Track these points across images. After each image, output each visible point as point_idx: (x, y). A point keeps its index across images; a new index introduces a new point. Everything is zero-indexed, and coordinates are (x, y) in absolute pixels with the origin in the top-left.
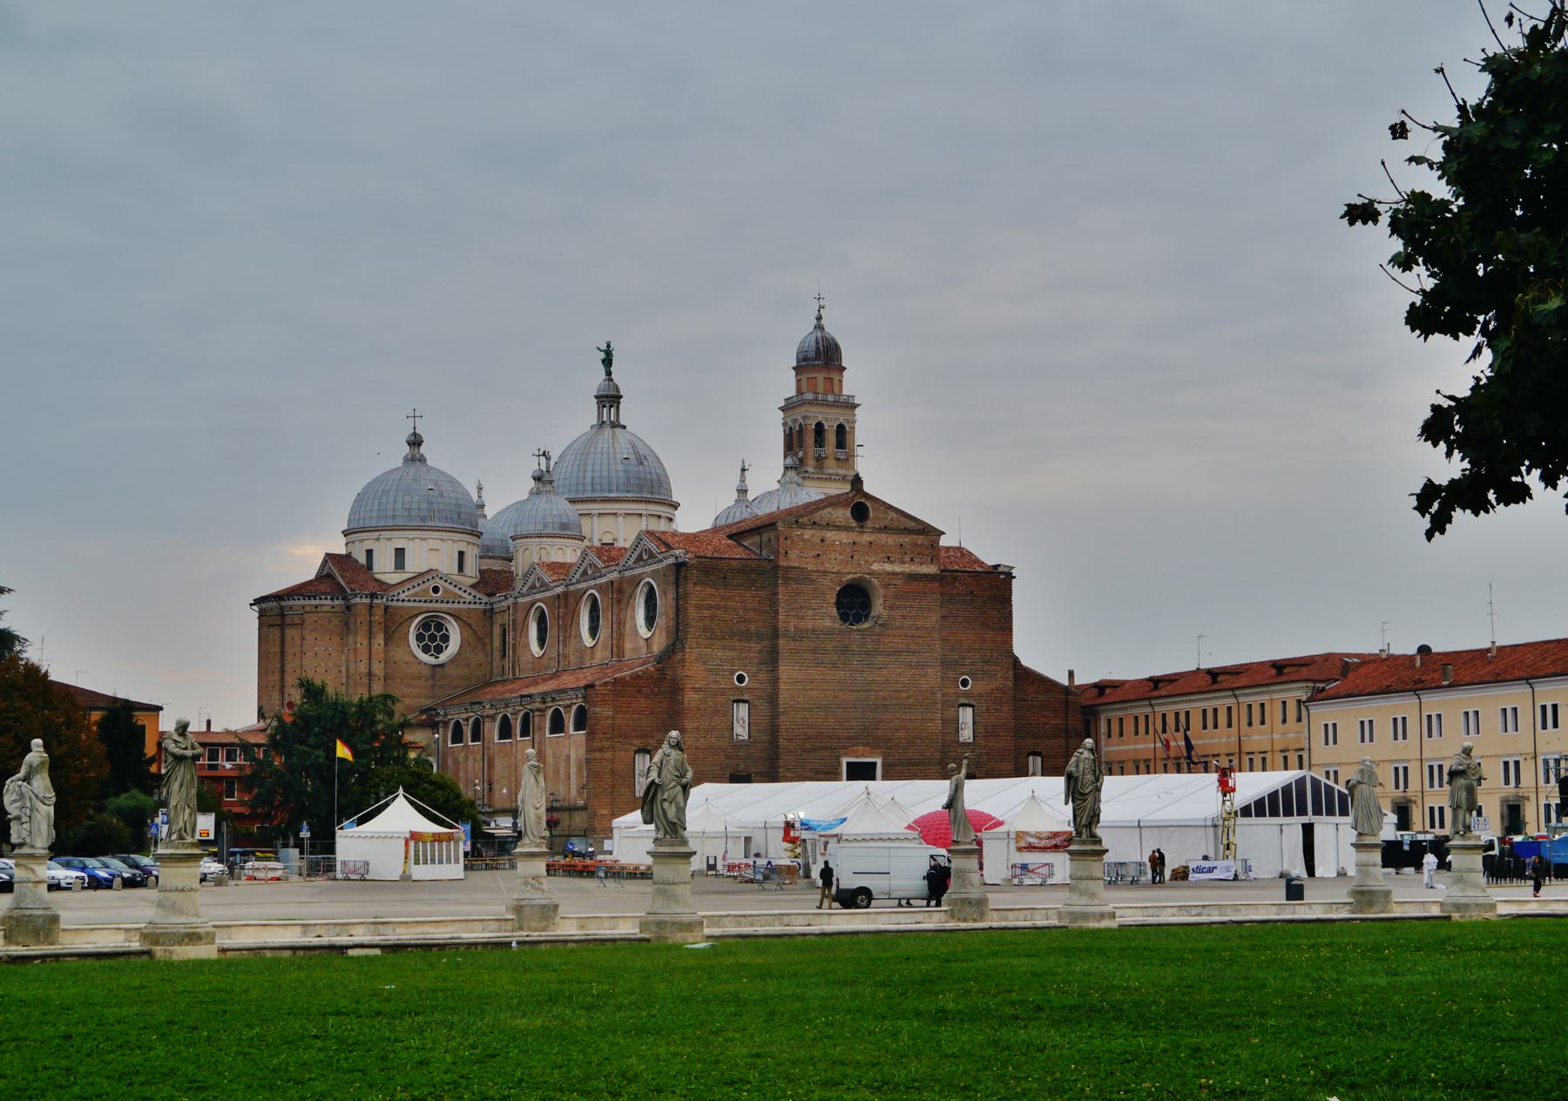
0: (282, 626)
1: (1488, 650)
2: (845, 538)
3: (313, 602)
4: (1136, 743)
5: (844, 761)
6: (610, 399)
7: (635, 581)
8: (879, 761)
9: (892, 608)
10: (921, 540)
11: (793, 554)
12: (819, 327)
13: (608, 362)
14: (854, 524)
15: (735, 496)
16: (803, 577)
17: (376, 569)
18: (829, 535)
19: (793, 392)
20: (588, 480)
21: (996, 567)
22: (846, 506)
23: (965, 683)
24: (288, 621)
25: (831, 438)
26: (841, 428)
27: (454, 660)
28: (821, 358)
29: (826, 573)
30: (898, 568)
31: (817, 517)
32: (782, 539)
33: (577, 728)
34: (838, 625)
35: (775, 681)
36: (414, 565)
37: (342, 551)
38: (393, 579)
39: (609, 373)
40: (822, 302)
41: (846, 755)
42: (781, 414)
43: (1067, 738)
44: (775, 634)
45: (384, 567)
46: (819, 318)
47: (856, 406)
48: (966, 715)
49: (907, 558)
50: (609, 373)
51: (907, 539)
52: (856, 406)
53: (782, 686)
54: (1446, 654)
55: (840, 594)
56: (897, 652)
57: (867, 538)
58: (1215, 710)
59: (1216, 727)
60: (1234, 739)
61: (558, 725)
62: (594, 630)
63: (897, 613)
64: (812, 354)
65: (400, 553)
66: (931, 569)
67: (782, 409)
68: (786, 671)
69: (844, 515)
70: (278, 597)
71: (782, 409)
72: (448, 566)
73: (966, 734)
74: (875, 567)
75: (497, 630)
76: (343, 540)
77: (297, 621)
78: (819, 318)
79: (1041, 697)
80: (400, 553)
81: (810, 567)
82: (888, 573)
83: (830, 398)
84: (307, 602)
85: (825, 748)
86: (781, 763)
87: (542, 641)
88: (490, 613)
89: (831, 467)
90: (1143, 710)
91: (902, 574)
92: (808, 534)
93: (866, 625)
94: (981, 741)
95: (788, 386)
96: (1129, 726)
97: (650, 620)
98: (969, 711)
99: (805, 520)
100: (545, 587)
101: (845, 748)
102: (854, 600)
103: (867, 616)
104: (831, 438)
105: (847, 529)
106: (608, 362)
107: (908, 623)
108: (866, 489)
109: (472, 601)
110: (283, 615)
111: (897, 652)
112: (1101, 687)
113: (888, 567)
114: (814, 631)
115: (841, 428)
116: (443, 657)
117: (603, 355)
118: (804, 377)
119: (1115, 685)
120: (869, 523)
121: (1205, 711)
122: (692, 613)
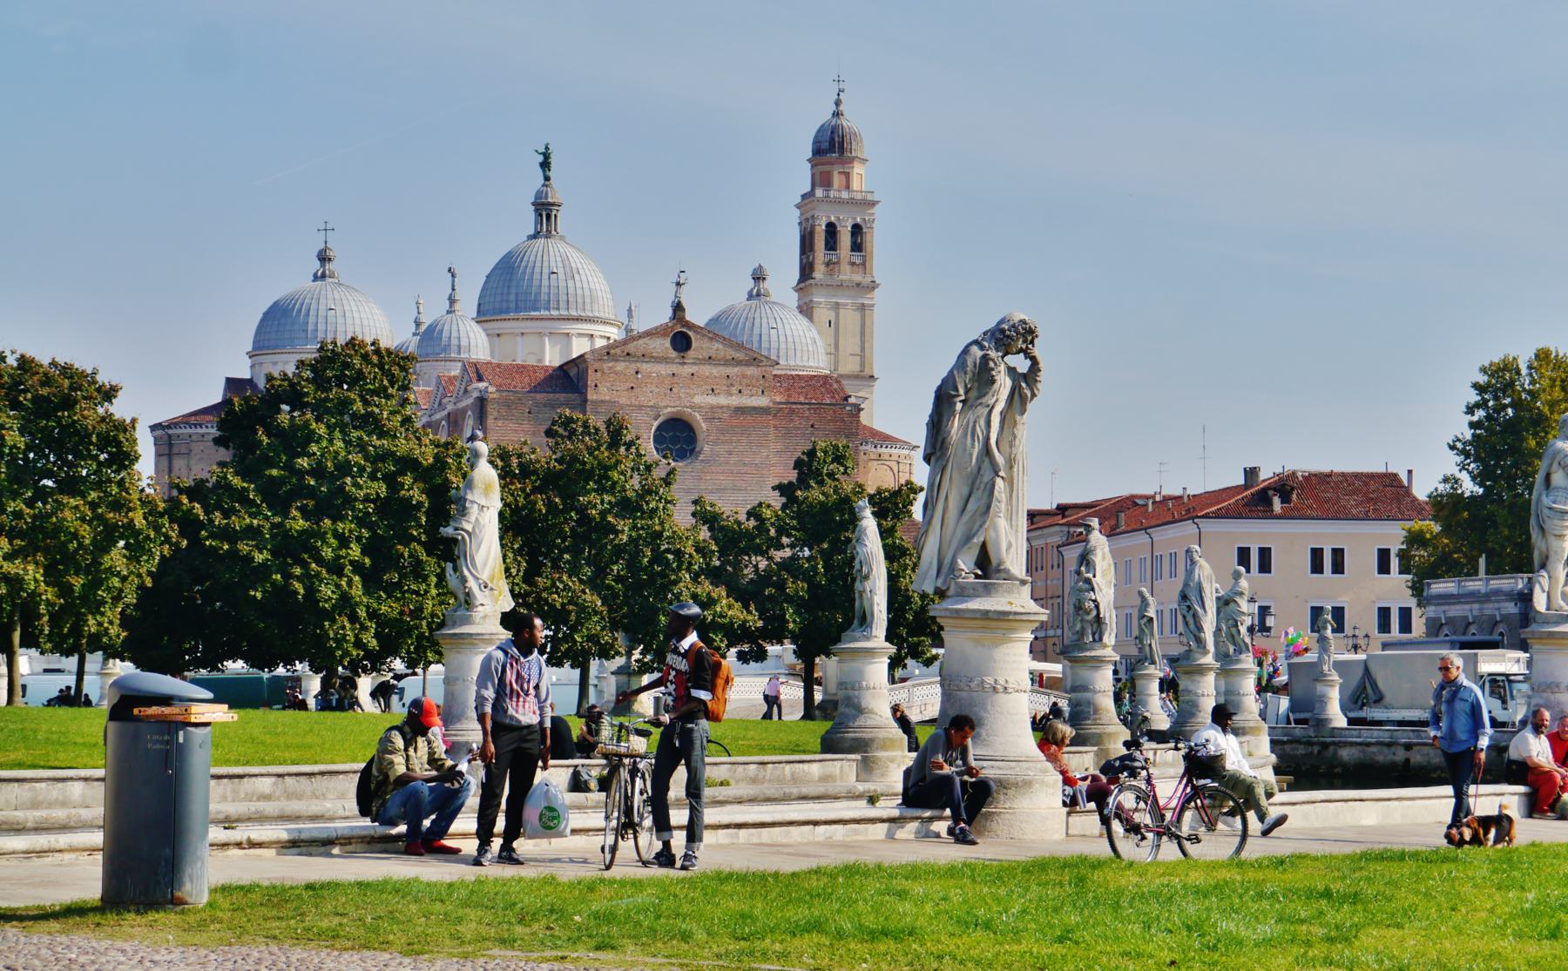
0: (170, 456)
1: (1181, 497)
2: (664, 369)
3: (199, 430)
6: (544, 210)
9: (715, 443)
10: (751, 371)
11: (600, 388)
12: (837, 114)
13: (545, 165)
14: (673, 354)
15: (669, 313)
18: (645, 367)
20: (512, 297)
24: (175, 450)
25: (845, 239)
26: (857, 230)
28: (832, 147)
29: (640, 407)
30: (723, 400)
31: (631, 348)
32: (590, 372)
37: (244, 373)
39: (547, 179)
40: (842, 86)
42: (797, 212)
46: (838, 103)
47: (873, 204)
49: (734, 390)
50: (547, 179)
51: (733, 371)
52: (873, 204)
57: (688, 369)
63: (721, 449)
64: (825, 145)
67: (798, 206)
69: (663, 345)
70: (172, 424)
71: (798, 206)
74: (698, 400)
76: (249, 362)
77: (184, 451)
78: (838, 103)
81: (623, 401)
82: (712, 408)
83: (845, 195)
84: (193, 430)
89: (846, 274)
91: (728, 407)
92: (620, 366)
95: (802, 180)
99: (618, 351)
103: (692, 451)
104: (845, 239)
105: (664, 360)
106: (545, 165)
107: (733, 459)
110: (170, 445)
115: (857, 230)
117: (541, 158)
118: (821, 168)
120: (691, 353)
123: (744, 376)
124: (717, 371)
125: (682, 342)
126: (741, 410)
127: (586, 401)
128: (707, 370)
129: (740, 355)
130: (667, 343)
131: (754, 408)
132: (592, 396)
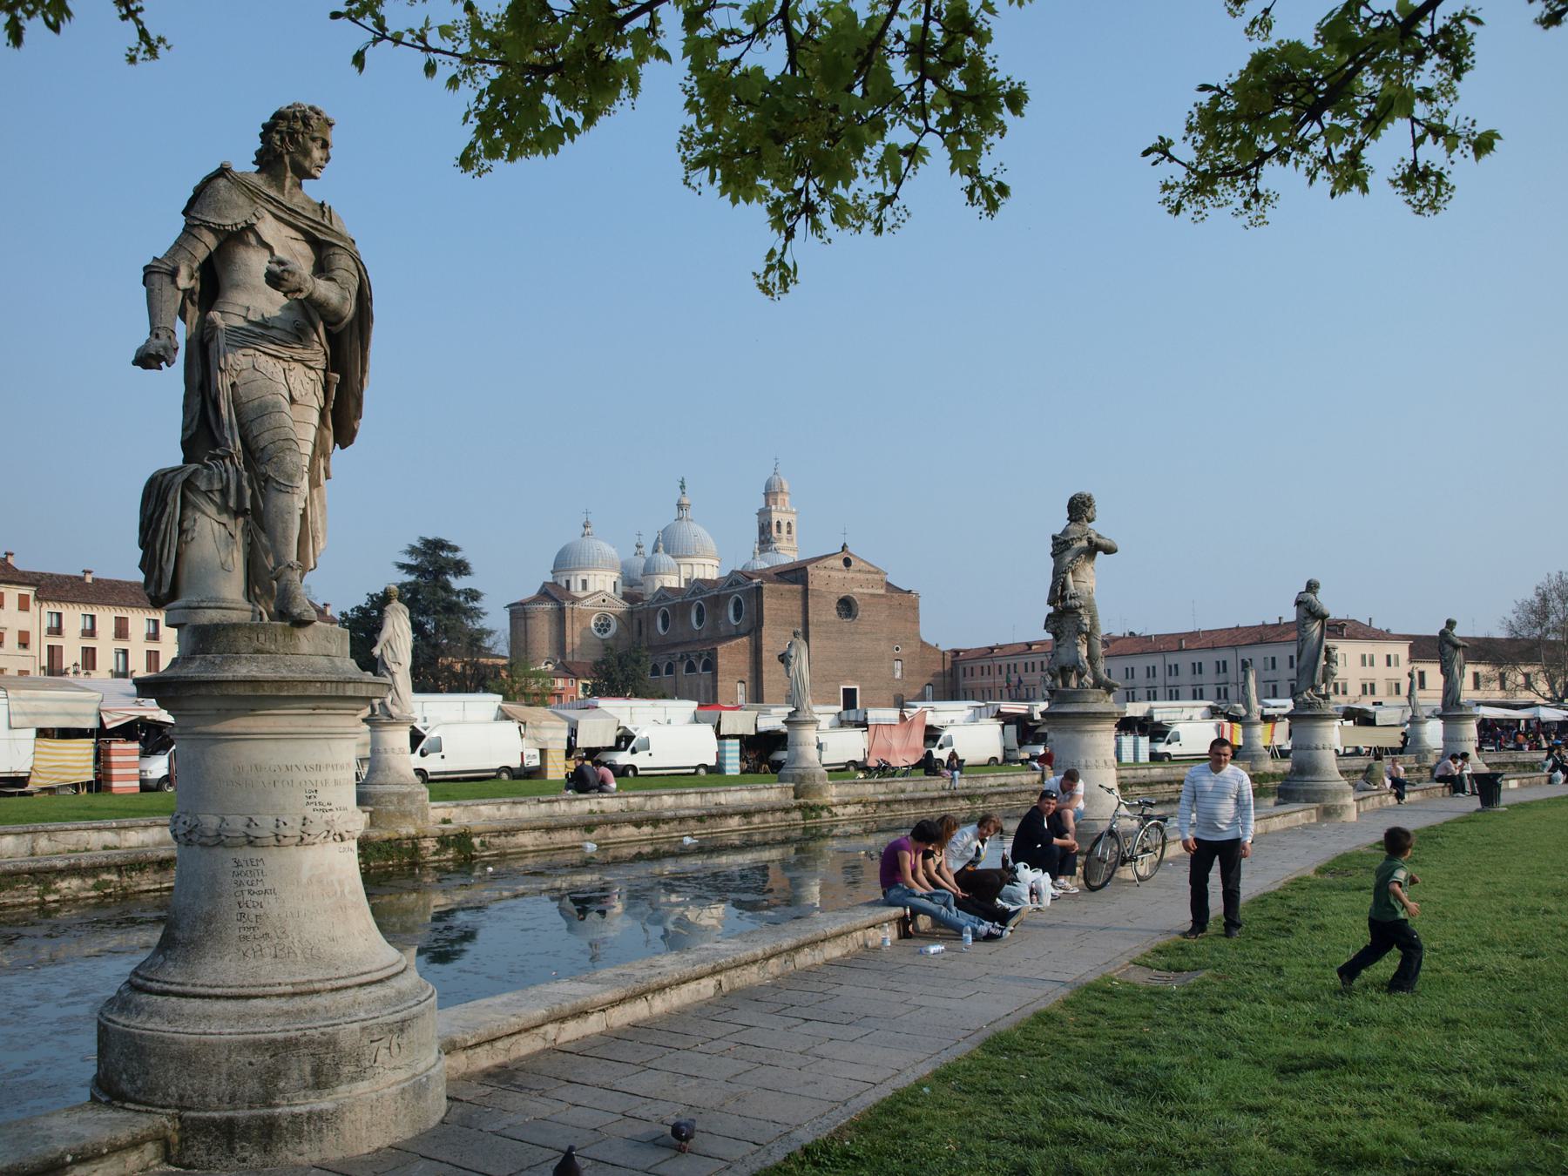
2: (841, 575)
7: (728, 596)
10: (877, 577)
13: (682, 487)
16: (821, 595)
17: (572, 589)
18: (833, 573)
19: (763, 506)
25: (784, 528)
27: (616, 637)
33: (704, 669)
34: (838, 619)
36: (591, 588)
38: (581, 594)
45: (576, 588)
57: (850, 575)
61: (691, 668)
62: (700, 621)
65: (584, 582)
66: (882, 592)
69: (840, 563)
70: (522, 604)
72: (610, 589)
73: (898, 675)
75: (635, 622)
80: (584, 582)
87: (665, 627)
88: (631, 613)
90: (986, 663)
96: (977, 671)
97: (737, 617)
100: (666, 599)
106: (682, 487)
108: (850, 549)
109: (621, 607)
112: (957, 652)
116: (607, 635)
122: (765, 612)
125: (847, 562)
126: (873, 595)
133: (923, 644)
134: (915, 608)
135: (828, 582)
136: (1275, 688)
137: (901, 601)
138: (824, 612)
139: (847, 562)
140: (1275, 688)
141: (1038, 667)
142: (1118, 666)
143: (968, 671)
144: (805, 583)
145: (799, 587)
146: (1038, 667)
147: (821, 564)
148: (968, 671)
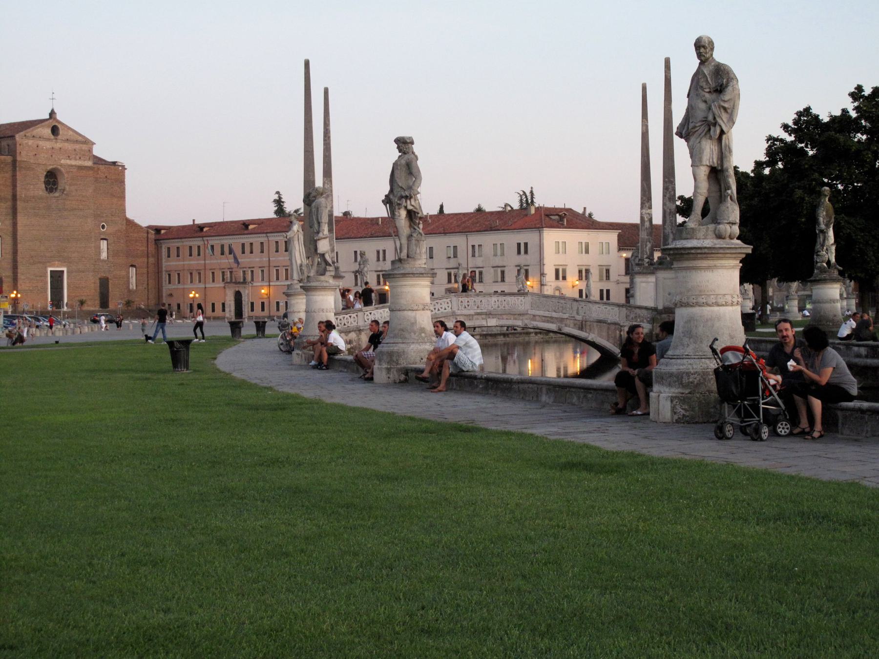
2: (47, 145)
4: (198, 260)
5: (49, 269)
8: (65, 269)
10: (84, 147)
11: (24, 153)
14: (52, 137)
18: (41, 143)
21: (114, 163)
22: (48, 127)
23: (103, 227)
30: (73, 162)
35: (15, 225)
41: (50, 266)
43: (148, 257)
44: (14, 198)
48: (104, 245)
51: (77, 146)
53: (19, 228)
54: (359, 219)
55: (46, 176)
56: (73, 209)
57: (58, 145)
58: (251, 244)
59: (251, 252)
60: (265, 259)
66: (89, 163)
68: (21, 220)
73: (104, 255)
74: (63, 162)
79: (135, 235)
85: (40, 262)
86: (19, 271)
90: (196, 242)
92: (30, 142)
93: (57, 194)
94: (110, 258)
98: (105, 242)
101: (49, 262)
102: (52, 178)
103: (56, 189)
105: (49, 140)
108: (59, 117)
111: (73, 209)
113: (69, 162)
114: (34, 197)
119: (168, 229)
120: (59, 137)
121: (243, 245)
123: (82, 150)
124: (69, 146)
125: (55, 130)
126: (80, 168)
127: (14, 161)
128: (66, 144)
129: (80, 138)
130: (49, 131)
131: (86, 167)
132: (18, 158)
133: (130, 223)
134: (121, 182)
135: (35, 151)
136: (503, 273)
137: (110, 176)
138: (32, 186)
139: (55, 130)
140: (503, 273)
141: (257, 248)
142: (346, 250)
143: (174, 252)
144: (12, 152)
145: (9, 159)
146: (257, 248)
147: (30, 132)
148: (174, 252)
